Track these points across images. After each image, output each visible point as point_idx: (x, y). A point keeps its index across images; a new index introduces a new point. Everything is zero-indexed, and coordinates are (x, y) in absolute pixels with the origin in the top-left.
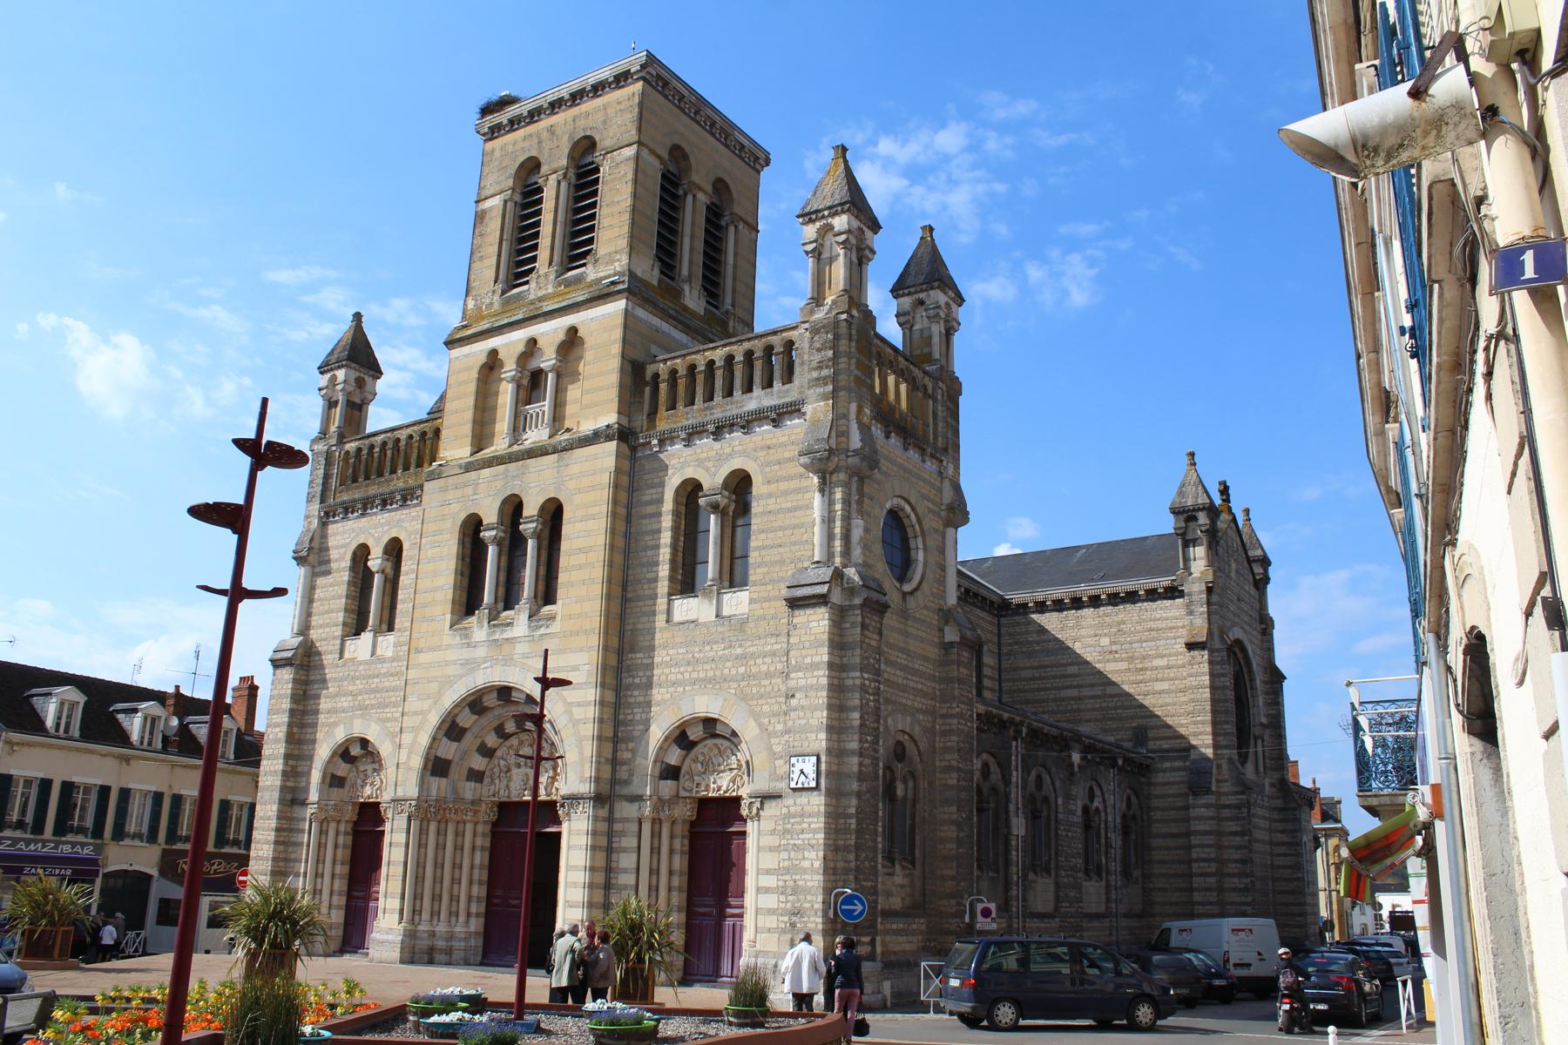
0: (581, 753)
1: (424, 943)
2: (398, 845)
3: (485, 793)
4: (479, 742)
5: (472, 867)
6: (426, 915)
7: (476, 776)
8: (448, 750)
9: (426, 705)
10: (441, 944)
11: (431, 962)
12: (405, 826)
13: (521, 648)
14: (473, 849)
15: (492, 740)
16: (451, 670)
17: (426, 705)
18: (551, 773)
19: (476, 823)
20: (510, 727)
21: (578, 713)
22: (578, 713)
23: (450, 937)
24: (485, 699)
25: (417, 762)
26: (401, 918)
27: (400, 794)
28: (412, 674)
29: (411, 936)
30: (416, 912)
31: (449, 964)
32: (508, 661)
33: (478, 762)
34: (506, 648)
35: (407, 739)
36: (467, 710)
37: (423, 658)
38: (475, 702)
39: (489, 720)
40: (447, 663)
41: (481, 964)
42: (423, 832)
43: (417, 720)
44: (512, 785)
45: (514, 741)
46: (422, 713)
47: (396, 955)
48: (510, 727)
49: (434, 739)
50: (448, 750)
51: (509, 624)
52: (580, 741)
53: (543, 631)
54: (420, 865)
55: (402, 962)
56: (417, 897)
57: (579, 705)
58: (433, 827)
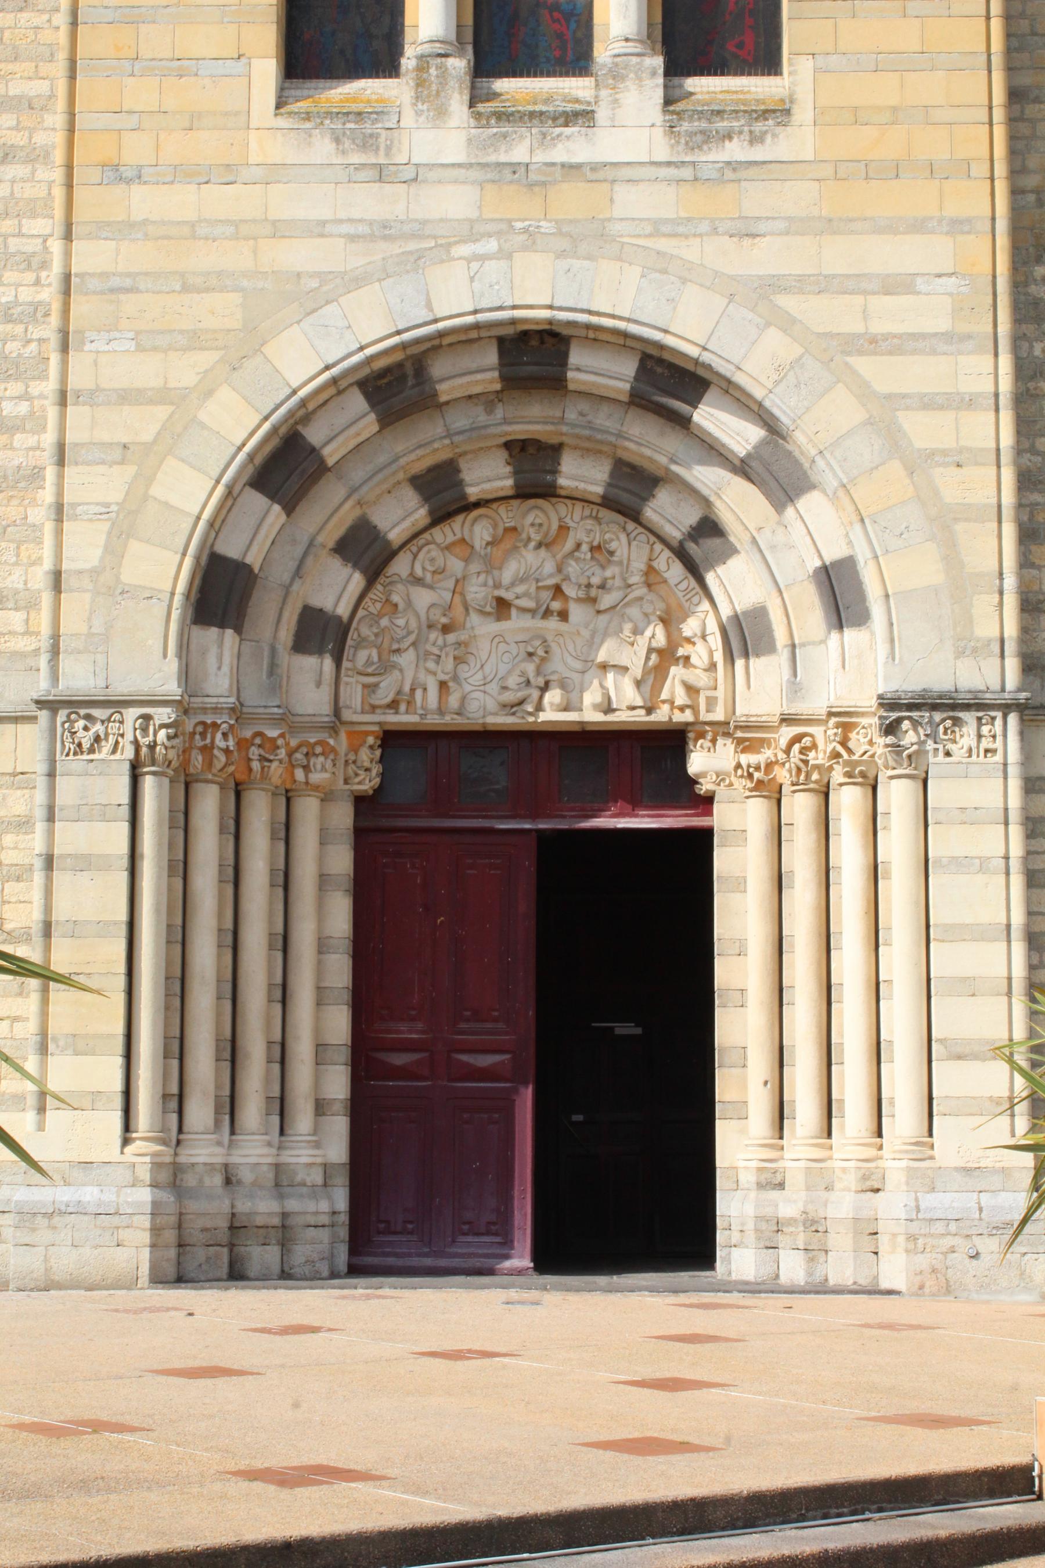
0: (951, 557)
1: (211, 1209)
2: (85, 863)
3: (353, 695)
4: (358, 512)
5: (322, 946)
6: (200, 1112)
7: (320, 633)
8: (260, 533)
9: (185, 370)
10: (264, 1208)
11: (236, 1274)
12: (124, 797)
13: (636, 203)
14: (324, 880)
15: (399, 515)
16: (299, 256)
17: (185, 370)
18: (661, 640)
19: (327, 797)
20: (488, 475)
21: (923, 430)
22: (923, 430)
23: (281, 1179)
24: (439, 368)
25: (164, 571)
26: (127, 1126)
27: (79, 677)
28: (91, 256)
29: (172, 1178)
30: (175, 1100)
31: (286, 1275)
32: (587, 239)
33: (336, 588)
34: (571, 200)
35: (94, 485)
36: (357, 402)
37: (142, 202)
38: (395, 384)
39: (420, 444)
40: (280, 230)
41: (355, 1270)
42: (181, 821)
43: (144, 424)
44: (472, 676)
45: (479, 530)
46: (162, 396)
47: (135, 1251)
48: (488, 475)
49: (229, 492)
50: (260, 533)
51: (570, 118)
52: (944, 524)
53: (736, 150)
54: (179, 937)
55: (158, 1279)
56: (176, 1048)
57: (929, 403)
58: (209, 805)
